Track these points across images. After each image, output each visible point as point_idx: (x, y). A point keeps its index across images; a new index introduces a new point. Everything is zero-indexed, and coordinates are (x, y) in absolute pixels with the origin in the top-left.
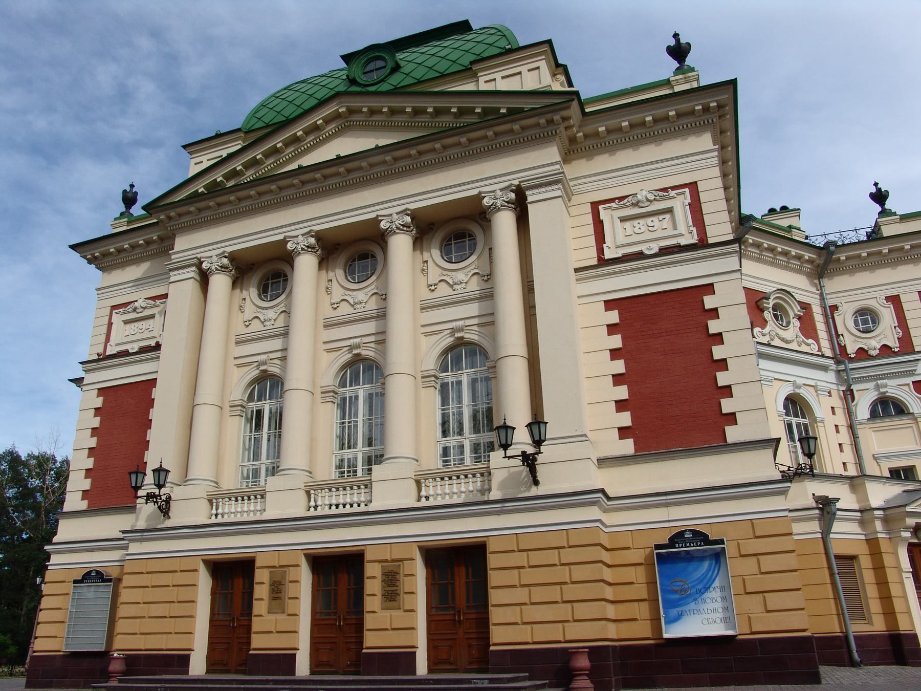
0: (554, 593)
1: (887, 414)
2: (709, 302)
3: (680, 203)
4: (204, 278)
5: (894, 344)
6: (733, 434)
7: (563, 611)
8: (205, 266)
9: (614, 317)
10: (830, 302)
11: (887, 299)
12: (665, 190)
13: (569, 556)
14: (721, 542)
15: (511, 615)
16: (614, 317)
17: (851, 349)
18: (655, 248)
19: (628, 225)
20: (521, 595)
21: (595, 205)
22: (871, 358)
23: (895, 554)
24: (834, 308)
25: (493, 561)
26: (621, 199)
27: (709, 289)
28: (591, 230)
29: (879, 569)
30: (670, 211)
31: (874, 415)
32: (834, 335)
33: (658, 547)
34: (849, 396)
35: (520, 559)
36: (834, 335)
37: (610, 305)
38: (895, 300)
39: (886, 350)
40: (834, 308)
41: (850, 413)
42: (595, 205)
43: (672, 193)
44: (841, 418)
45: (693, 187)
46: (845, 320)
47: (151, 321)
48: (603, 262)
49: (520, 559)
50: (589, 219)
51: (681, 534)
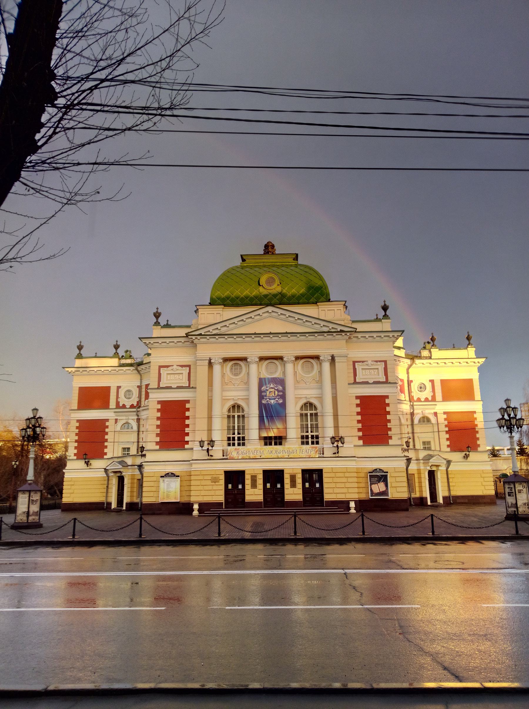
0: (342, 485)
1: (424, 421)
2: (387, 401)
3: (381, 366)
6: (391, 442)
7: (345, 490)
9: (358, 402)
10: (410, 379)
11: (431, 381)
12: (377, 361)
13: (347, 475)
14: (387, 472)
15: (330, 491)
16: (358, 402)
19: (364, 371)
20: (333, 485)
21: (354, 363)
22: (421, 401)
23: (424, 473)
24: (412, 381)
25: (325, 475)
26: (363, 362)
27: (387, 397)
28: (352, 371)
29: (420, 478)
30: (378, 369)
31: (420, 421)
32: (410, 392)
33: (369, 473)
35: (332, 475)
36: (410, 392)
37: (357, 397)
38: (432, 381)
40: (412, 381)
42: (354, 363)
43: (379, 363)
44: (409, 422)
45: (385, 362)
46: (414, 387)
47: (181, 376)
48: (355, 382)
49: (332, 475)
50: (352, 367)
51: (376, 469)
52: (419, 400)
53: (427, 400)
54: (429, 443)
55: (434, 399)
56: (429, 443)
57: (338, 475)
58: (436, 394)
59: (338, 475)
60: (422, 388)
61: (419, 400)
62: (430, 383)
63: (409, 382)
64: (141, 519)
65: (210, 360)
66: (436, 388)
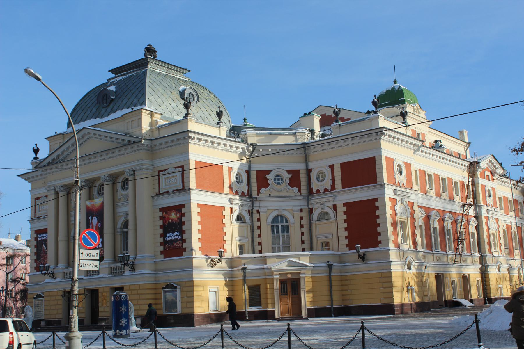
4: (57, 193)
5: (329, 188)
8: (56, 189)
12: (175, 168)
13: (140, 292)
17: (314, 190)
18: (171, 190)
26: (165, 170)
30: (176, 176)
32: (309, 183)
34: (311, 211)
38: (332, 167)
39: (326, 190)
41: (310, 219)
46: (314, 176)
48: (160, 194)
52: (318, 191)
53: (326, 190)
54: (328, 243)
55: (333, 187)
56: (328, 243)
57: (134, 292)
58: (336, 182)
59: (134, 292)
60: (321, 177)
61: (318, 191)
62: (330, 170)
63: (309, 172)
64: (103, 333)
65: (55, 188)
66: (336, 174)
